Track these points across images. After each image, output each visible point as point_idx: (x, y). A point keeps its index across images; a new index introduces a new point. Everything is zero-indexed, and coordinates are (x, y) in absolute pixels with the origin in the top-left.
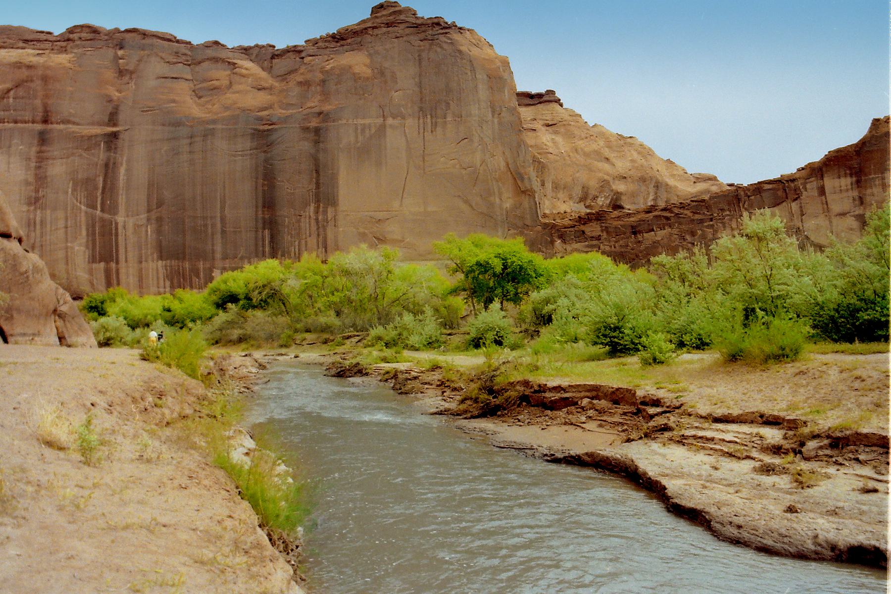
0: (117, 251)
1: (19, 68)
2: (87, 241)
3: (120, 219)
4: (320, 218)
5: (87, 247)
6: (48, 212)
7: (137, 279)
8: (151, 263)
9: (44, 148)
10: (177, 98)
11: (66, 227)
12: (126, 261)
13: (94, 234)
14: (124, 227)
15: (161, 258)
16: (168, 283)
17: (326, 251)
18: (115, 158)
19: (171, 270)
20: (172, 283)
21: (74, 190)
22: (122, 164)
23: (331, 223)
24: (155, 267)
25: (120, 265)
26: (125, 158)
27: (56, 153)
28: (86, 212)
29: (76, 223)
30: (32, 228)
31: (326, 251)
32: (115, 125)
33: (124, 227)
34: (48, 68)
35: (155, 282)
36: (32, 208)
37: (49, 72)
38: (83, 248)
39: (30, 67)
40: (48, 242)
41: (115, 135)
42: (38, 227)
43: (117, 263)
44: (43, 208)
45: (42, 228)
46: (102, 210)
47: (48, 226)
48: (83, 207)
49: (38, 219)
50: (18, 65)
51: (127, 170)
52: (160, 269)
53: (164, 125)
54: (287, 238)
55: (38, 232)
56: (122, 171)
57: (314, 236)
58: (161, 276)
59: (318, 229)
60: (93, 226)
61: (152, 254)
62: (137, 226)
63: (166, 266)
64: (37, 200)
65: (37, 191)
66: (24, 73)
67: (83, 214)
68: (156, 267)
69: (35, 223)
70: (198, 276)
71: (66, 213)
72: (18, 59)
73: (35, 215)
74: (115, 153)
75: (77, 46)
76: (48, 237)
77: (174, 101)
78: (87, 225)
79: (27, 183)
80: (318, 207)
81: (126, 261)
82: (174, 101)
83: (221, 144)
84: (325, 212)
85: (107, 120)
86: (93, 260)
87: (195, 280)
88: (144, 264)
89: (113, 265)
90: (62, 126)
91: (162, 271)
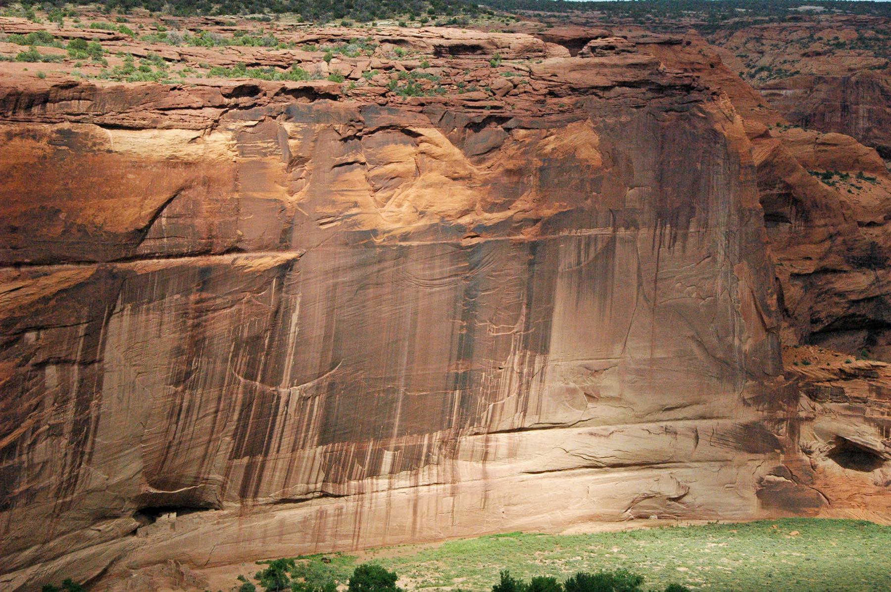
0: (270, 438)
1: (175, 166)
2: (237, 428)
3: (283, 391)
4: (525, 370)
5: (234, 436)
6: (200, 391)
7: (284, 474)
8: (307, 452)
9: (204, 295)
10: (359, 199)
11: (216, 412)
12: (278, 451)
13: (248, 416)
14: (287, 403)
15: (321, 442)
16: (322, 476)
17: (524, 416)
18: (287, 300)
19: (331, 456)
20: (327, 475)
21: (236, 355)
22: (294, 312)
23: (537, 378)
24: (312, 455)
25: (269, 458)
26: (299, 300)
27: (218, 301)
28: (245, 387)
29: (230, 404)
30: (174, 419)
31: (524, 416)
32: (287, 248)
33: (287, 403)
34: (212, 164)
35: (306, 477)
36: (180, 388)
37: (213, 172)
38: (228, 439)
39: (188, 164)
40: (189, 437)
41: (288, 266)
42: (182, 416)
43: (266, 455)
44: (193, 387)
45: (186, 417)
46: (262, 381)
47: (195, 412)
48: (242, 379)
49: (185, 404)
50: (172, 162)
51: (300, 317)
52: (318, 455)
53: (346, 244)
54: (481, 400)
55: (181, 423)
56: (295, 318)
57: (514, 395)
58: (317, 465)
59: (520, 386)
60: (251, 403)
61: (313, 437)
62: (303, 399)
63: (326, 452)
64: (188, 374)
65: (189, 363)
66: (179, 176)
67: (241, 389)
68: (314, 453)
69: (180, 410)
70: (363, 465)
71: (221, 390)
72: (168, 153)
73: (182, 399)
74: (286, 292)
75: (234, 118)
76: (191, 429)
77: (356, 204)
78: (243, 405)
79: (179, 351)
80: (524, 356)
81: (278, 451)
82: (356, 204)
83: (415, 268)
84: (532, 363)
85: (277, 241)
86: (236, 454)
87: (358, 468)
88: (299, 452)
89: (260, 458)
90: (227, 258)
91: (319, 460)
